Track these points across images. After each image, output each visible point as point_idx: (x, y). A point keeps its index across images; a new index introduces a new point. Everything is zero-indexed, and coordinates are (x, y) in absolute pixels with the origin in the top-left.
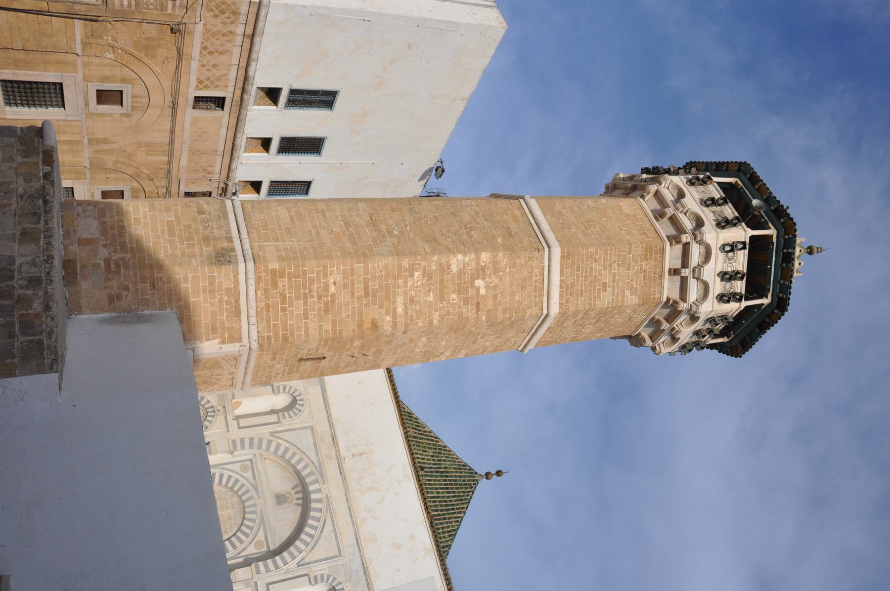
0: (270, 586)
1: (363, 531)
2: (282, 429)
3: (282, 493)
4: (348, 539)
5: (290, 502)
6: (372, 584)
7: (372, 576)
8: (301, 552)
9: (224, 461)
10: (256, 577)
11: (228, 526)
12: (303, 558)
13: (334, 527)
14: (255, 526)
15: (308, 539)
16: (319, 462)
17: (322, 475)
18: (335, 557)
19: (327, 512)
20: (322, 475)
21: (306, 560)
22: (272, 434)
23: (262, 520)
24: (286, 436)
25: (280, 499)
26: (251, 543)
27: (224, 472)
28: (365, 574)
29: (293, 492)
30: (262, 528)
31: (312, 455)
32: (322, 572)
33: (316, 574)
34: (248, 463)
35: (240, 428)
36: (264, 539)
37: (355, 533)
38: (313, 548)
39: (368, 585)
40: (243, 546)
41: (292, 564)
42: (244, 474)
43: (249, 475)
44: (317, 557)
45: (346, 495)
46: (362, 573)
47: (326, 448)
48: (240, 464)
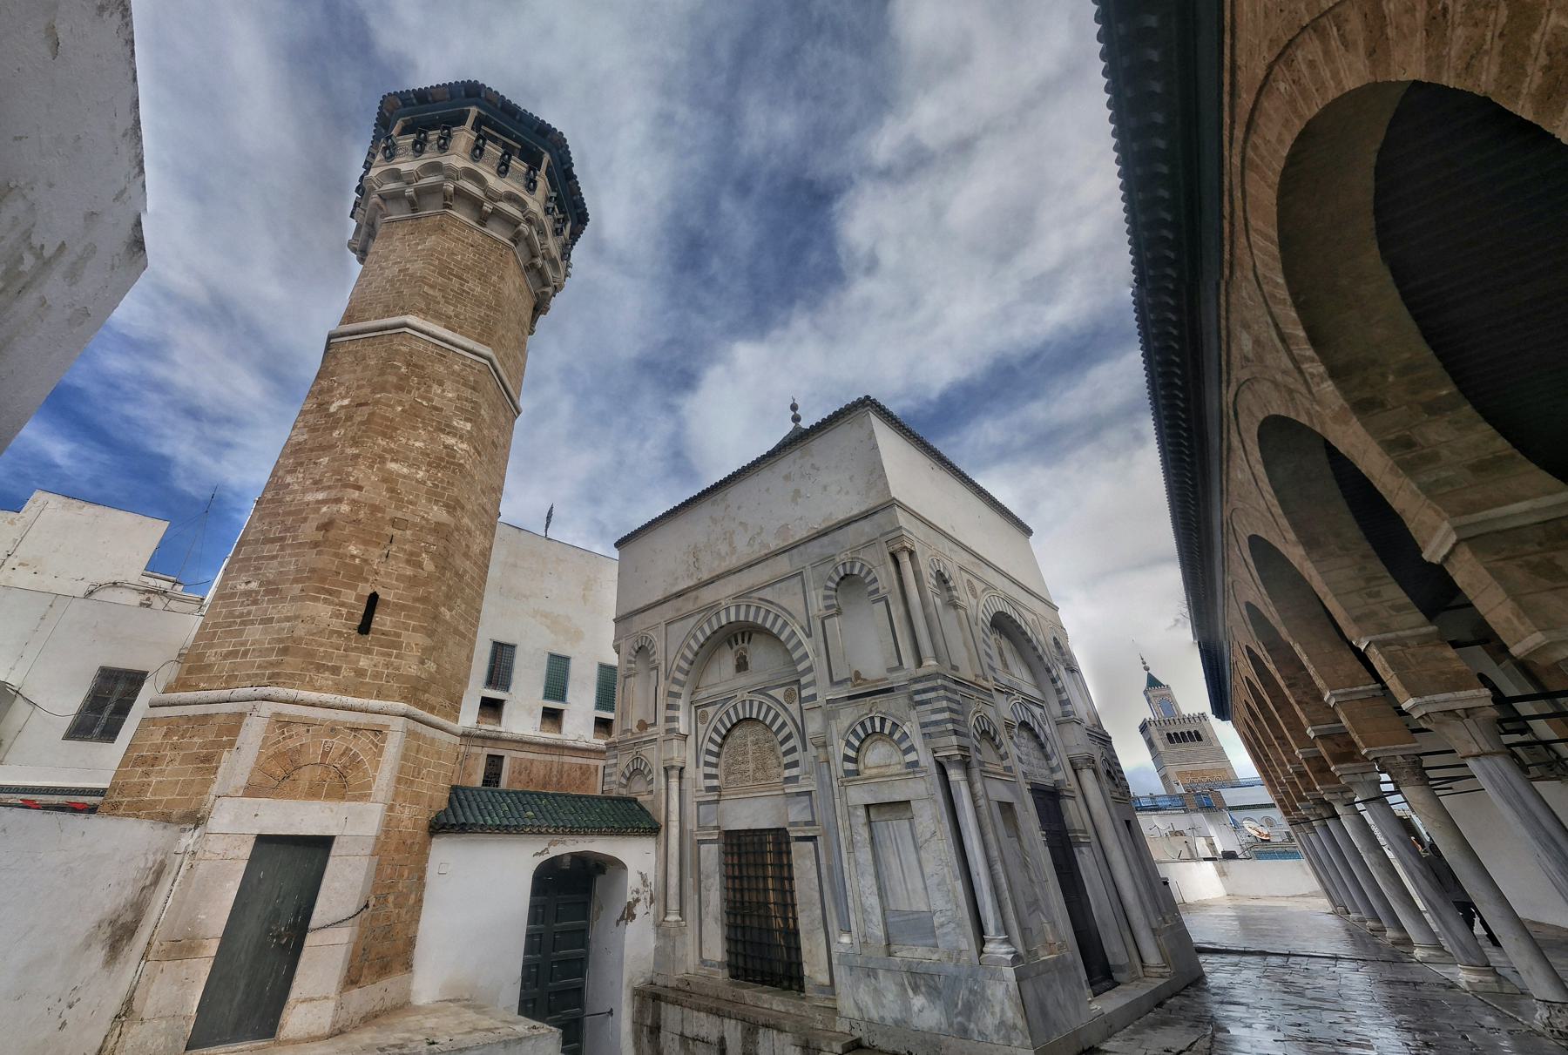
0: (835, 680)
1: (774, 544)
2: (663, 665)
3: (735, 663)
4: (783, 565)
5: (745, 650)
6: (839, 523)
7: (831, 523)
8: (793, 633)
9: (694, 746)
10: (820, 700)
11: (767, 745)
12: (802, 628)
13: (768, 585)
14: (767, 702)
15: (780, 622)
16: (698, 613)
17: (712, 607)
18: (803, 580)
19: (750, 598)
20: (712, 607)
21: (805, 624)
22: (666, 679)
23: (760, 692)
24: (671, 657)
25: (742, 665)
26: (786, 709)
27: (704, 748)
28: (826, 534)
29: (735, 648)
30: (771, 692)
31: (692, 621)
32: (820, 598)
33: (821, 607)
34: (699, 711)
35: (654, 724)
36: (784, 689)
37: (777, 555)
38: (790, 614)
39: (841, 528)
40: (789, 722)
41: (808, 646)
42: (710, 718)
43: (710, 710)
44: (801, 607)
45: (734, 573)
46: (825, 540)
47: (686, 605)
48: (699, 724)
